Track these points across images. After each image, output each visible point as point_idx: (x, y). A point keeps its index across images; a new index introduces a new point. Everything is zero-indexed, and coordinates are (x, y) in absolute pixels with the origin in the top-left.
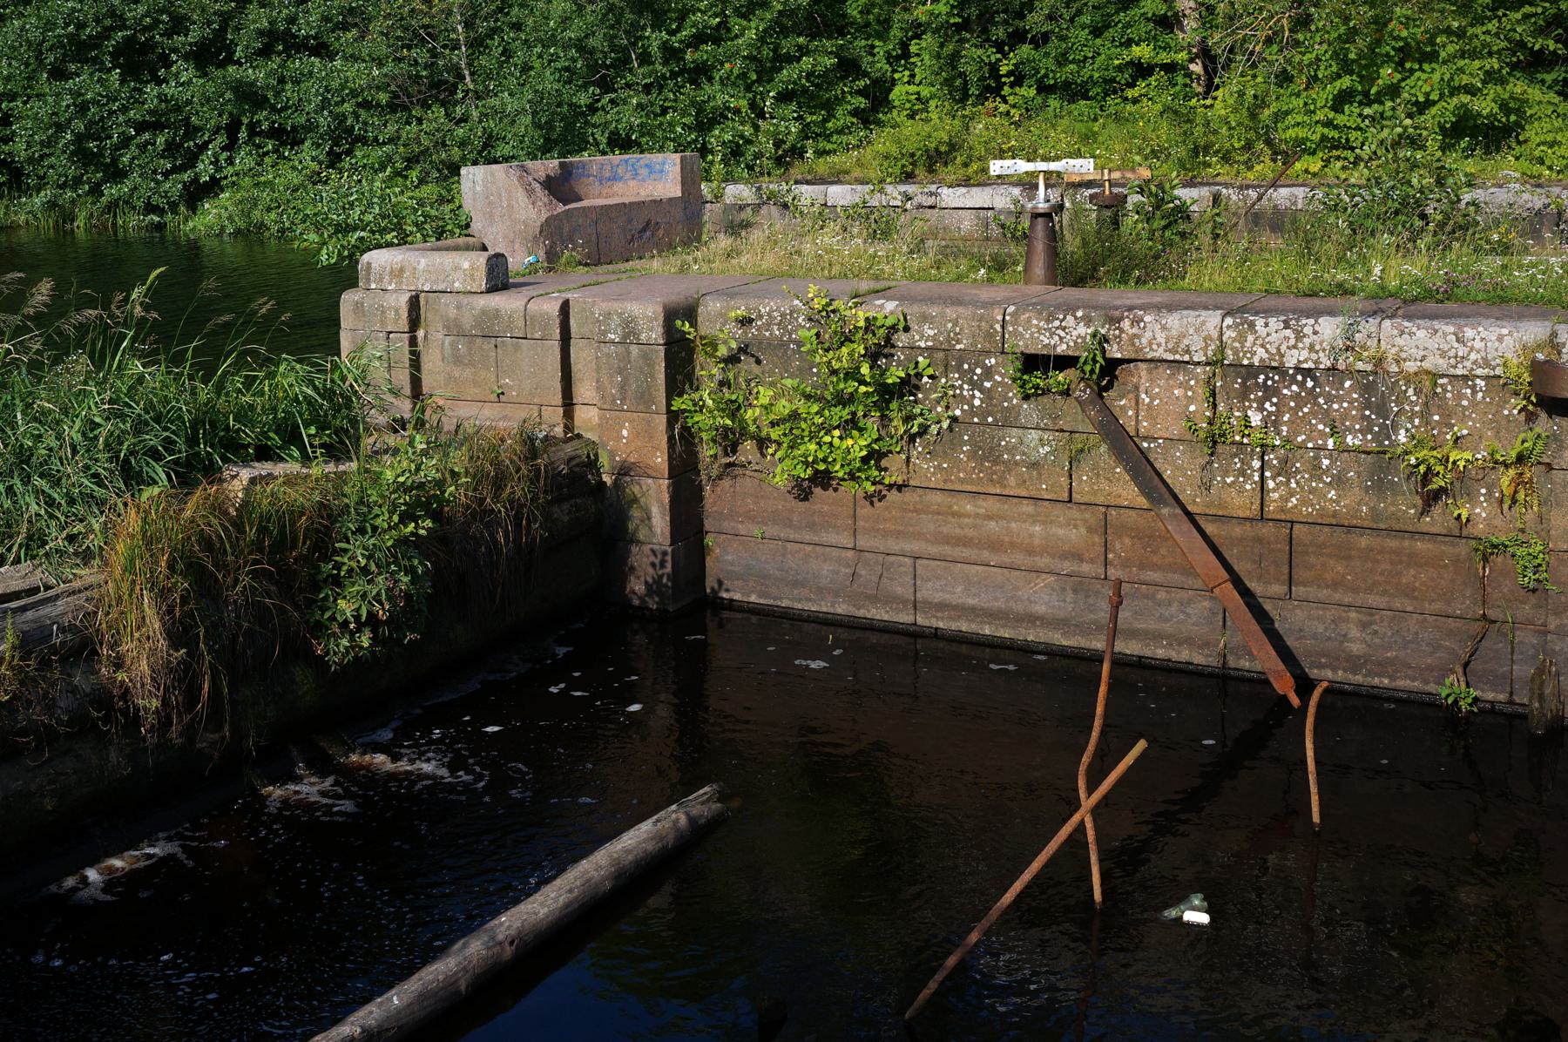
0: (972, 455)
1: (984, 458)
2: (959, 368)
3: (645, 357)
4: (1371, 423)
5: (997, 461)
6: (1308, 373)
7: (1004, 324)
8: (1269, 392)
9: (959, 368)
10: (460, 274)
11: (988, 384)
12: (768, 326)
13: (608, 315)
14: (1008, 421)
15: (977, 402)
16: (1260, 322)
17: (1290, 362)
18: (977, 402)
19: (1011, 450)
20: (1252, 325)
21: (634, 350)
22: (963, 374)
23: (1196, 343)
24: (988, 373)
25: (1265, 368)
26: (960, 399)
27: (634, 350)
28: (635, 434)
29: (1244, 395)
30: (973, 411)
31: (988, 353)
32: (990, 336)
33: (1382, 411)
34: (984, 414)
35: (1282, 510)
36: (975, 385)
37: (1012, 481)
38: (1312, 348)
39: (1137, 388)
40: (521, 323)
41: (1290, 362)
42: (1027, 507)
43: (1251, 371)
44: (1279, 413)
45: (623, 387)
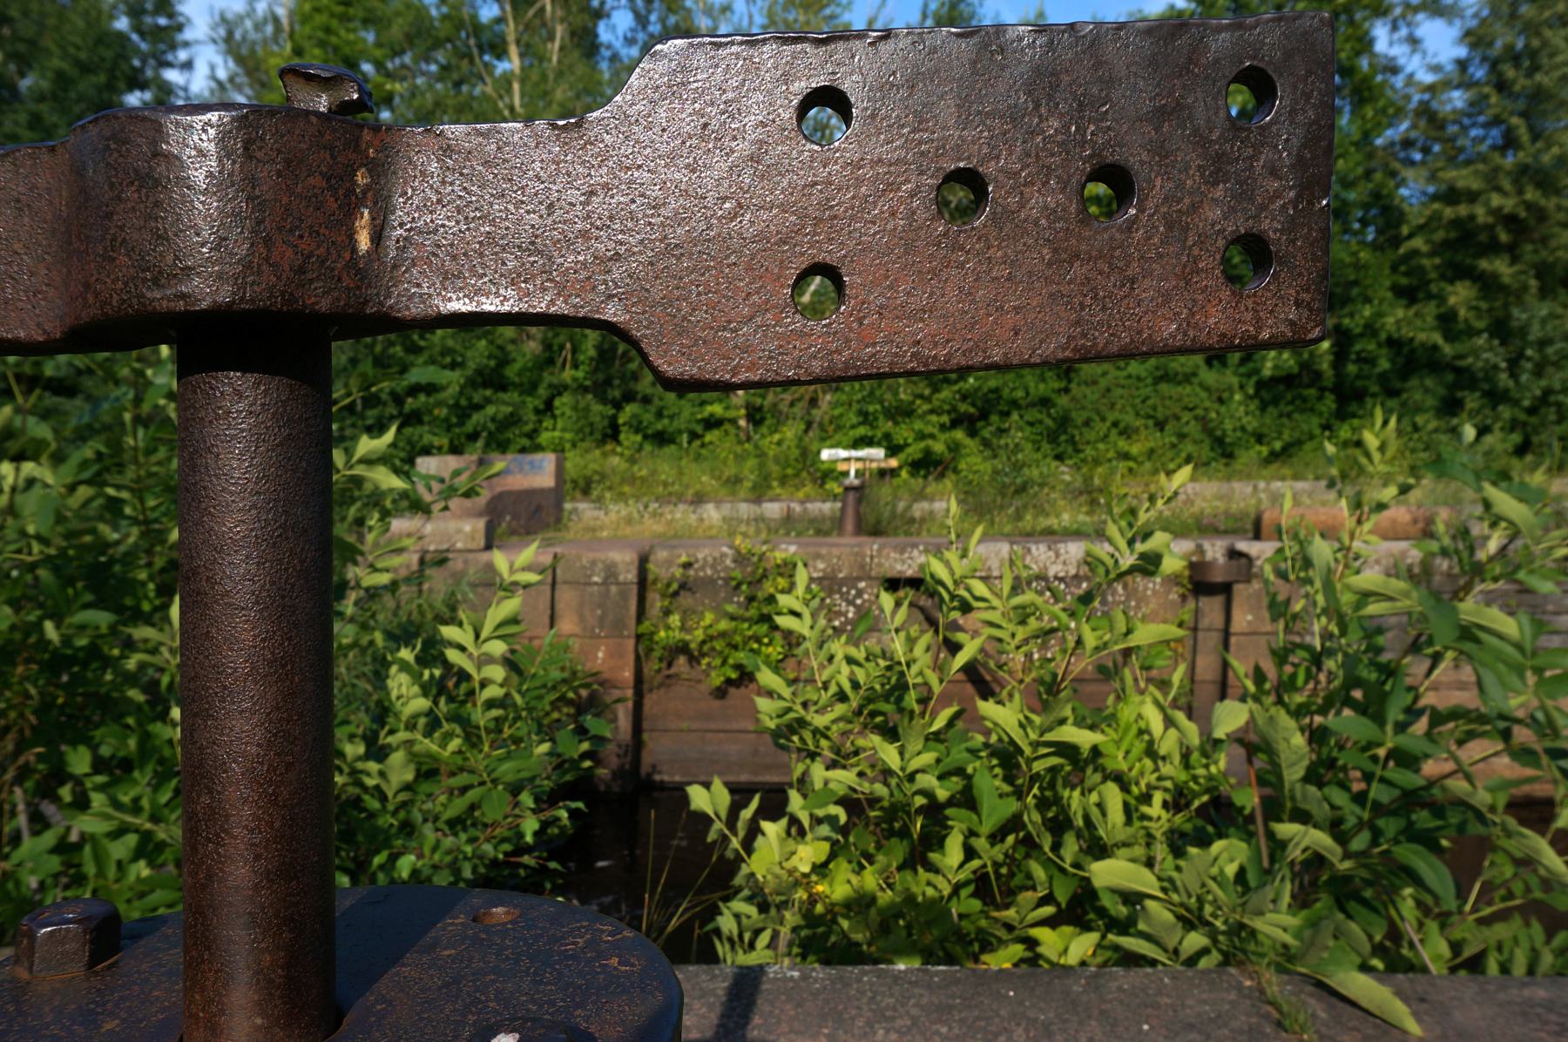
3: (623, 595)
6: (1061, 580)
7: (872, 557)
11: (859, 602)
12: (703, 568)
13: (593, 563)
15: (850, 615)
16: (1033, 548)
17: (1051, 573)
18: (850, 615)
20: (1029, 550)
21: (613, 589)
22: (842, 594)
24: (860, 593)
26: (839, 614)
27: (613, 589)
28: (610, 655)
30: (847, 622)
31: (860, 579)
32: (862, 566)
36: (851, 603)
38: (1064, 563)
41: (1051, 573)
45: (602, 619)
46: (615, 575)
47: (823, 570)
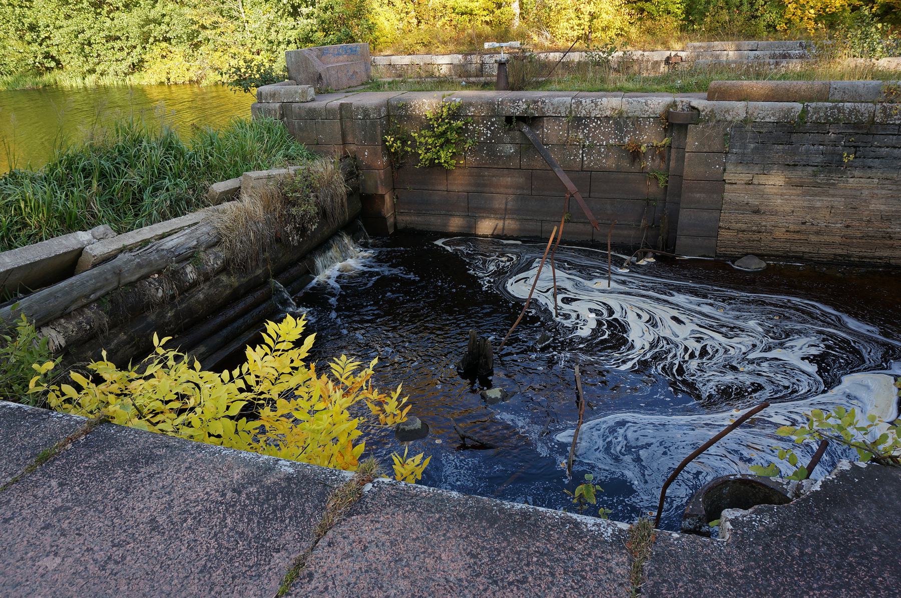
0: (487, 154)
1: (491, 155)
2: (483, 123)
4: (617, 135)
5: (496, 156)
6: (598, 118)
8: (586, 126)
9: (483, 123)
10: (298, 95)
14: (500, 141)
19: (500, 151)
23: (563, 110)
24: (493, 124)
25: (585, 118)
28: (370, 154)
29: (578, 127)
30: (487, 138)
33: (621, 131)
34: (490, 139)
35: (588, 167)
36: (488, 129)
37: (501, 162)
39: (542, 127)
40: (324, 113)
42: (506, 171)
43: (580, 119)
44: (589, 133)
46: (369, 115)
47: (474, 112)
